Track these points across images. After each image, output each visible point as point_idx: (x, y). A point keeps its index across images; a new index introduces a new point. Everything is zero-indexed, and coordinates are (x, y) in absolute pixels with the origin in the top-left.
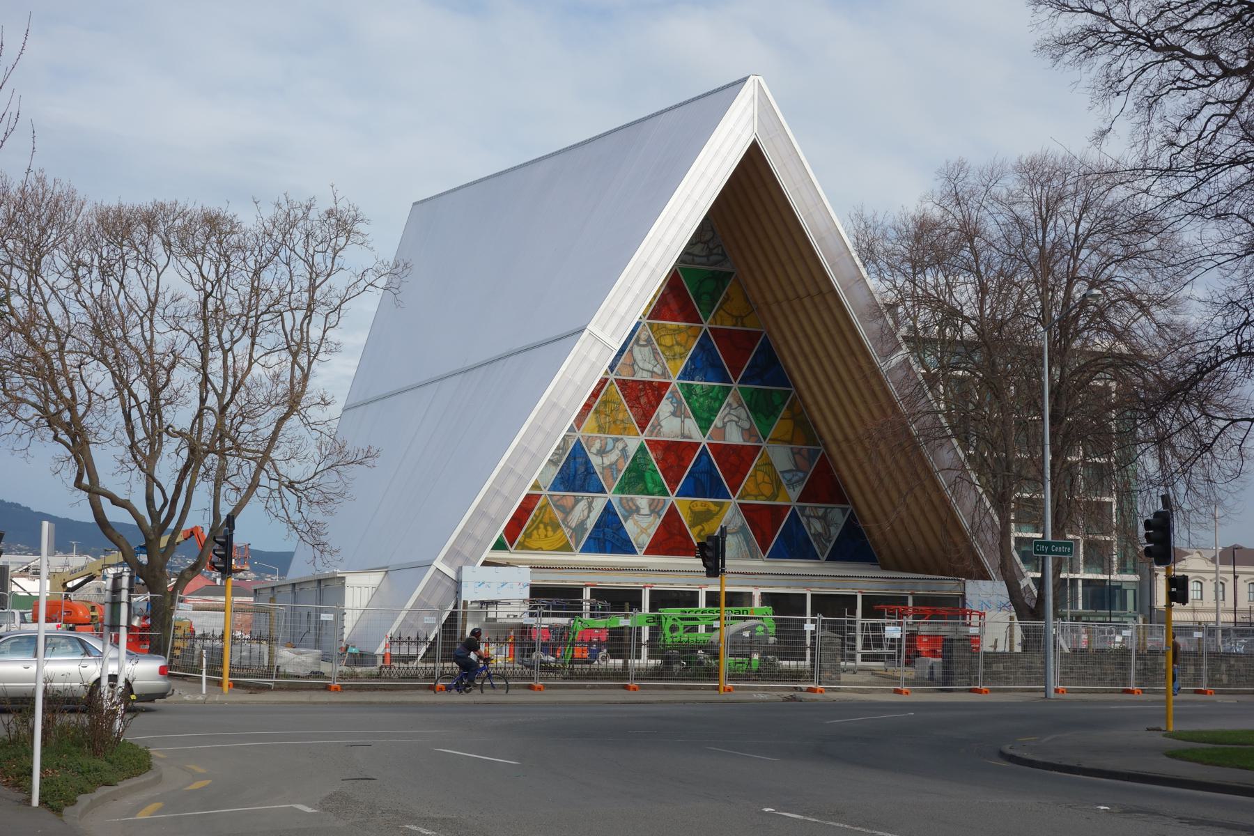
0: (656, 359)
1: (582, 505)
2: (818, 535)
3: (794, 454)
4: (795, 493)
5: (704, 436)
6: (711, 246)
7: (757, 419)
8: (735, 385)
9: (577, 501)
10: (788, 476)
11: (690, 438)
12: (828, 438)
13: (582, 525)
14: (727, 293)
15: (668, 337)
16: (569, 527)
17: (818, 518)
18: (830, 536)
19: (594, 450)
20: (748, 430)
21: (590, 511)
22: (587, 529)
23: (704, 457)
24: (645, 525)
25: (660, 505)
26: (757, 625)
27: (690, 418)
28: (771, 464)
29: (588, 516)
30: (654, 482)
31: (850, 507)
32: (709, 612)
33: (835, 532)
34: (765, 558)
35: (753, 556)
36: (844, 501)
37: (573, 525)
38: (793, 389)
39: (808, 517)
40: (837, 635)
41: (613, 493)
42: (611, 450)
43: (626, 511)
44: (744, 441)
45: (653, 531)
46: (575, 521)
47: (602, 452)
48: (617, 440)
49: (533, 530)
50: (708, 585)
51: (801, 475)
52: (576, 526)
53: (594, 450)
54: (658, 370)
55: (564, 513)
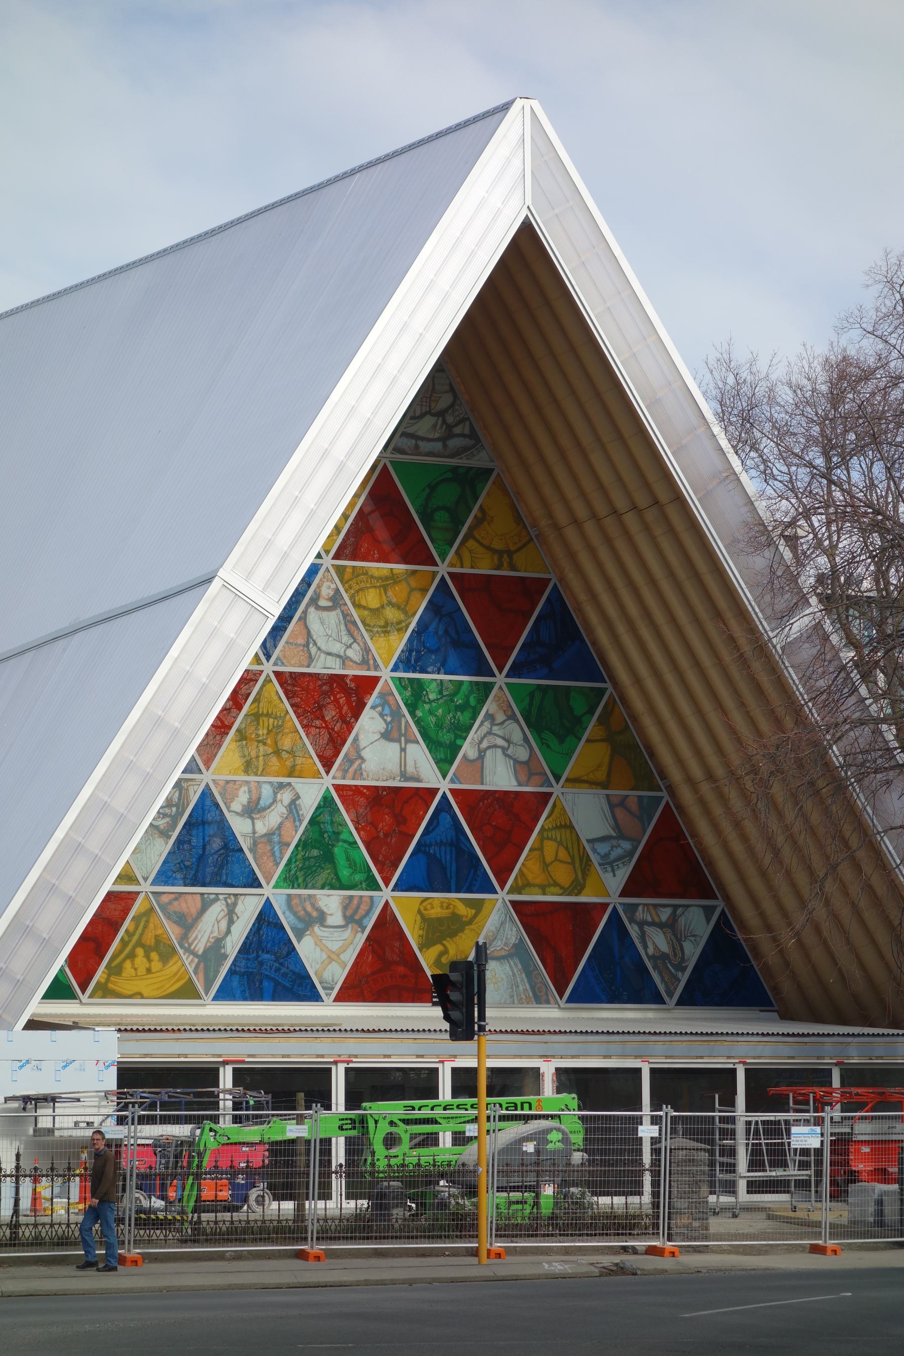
0: (350, 634)
1: (217, 910)
2: (660, 958)
3: (612, 807)
4: (615, 881)
5: (444, 777)
6: (450, 419)
7: (543, 743)
8: (500, 679)
9: (206, 904)
10: (603, 848)
11: (418, 780)
12: (676, 775)
13: (216, 947)
14: (481, 508)
15: (372, 591)
16: (195, 954)
17: (661, 926)
18: (683, 959)
19: (237, 806)
20: (526, 763)
21: (231, 922)
22: (225, 957)
23: (445, 818)
24: (335, 946)
25: (364, 908)
26: (549, 1131)
27: (418, 742)
28: (571, 827)
29: (228, 932)
30: (352, 864)
31: (720, 904)
32: (458, 1107)
33: (693, 951)
34: (562, 1003)
35: (539, 999)
36: (705, 892)
37: (200, 949)
38: (608, 685)
39: (641, 924)
40: (703, 1146)
41: (275, 887)
42: (269, 807)
44: (520, 785)
45: (350, 957)
46: (204, 940)
47: (253, 810)
48: (281, 786)
49: (124, 960)
50: (455, 1056)
51: (626, 845)
52: (205, 951)
53: (237, 806)
54: (354, 653)
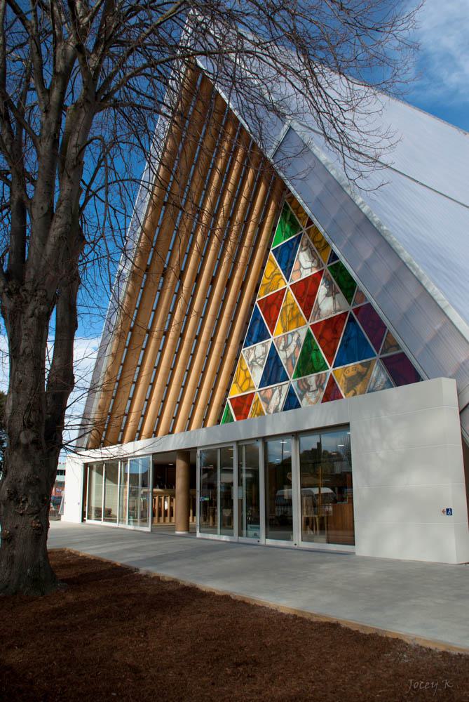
1: (277, 392)
19: (281, 348)
21: (280, 397)
29: (280, 402)
43: (302, 391)
47: (286, 347)
55: (266, 402)
